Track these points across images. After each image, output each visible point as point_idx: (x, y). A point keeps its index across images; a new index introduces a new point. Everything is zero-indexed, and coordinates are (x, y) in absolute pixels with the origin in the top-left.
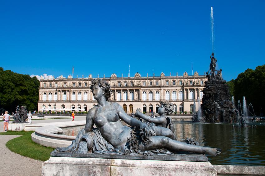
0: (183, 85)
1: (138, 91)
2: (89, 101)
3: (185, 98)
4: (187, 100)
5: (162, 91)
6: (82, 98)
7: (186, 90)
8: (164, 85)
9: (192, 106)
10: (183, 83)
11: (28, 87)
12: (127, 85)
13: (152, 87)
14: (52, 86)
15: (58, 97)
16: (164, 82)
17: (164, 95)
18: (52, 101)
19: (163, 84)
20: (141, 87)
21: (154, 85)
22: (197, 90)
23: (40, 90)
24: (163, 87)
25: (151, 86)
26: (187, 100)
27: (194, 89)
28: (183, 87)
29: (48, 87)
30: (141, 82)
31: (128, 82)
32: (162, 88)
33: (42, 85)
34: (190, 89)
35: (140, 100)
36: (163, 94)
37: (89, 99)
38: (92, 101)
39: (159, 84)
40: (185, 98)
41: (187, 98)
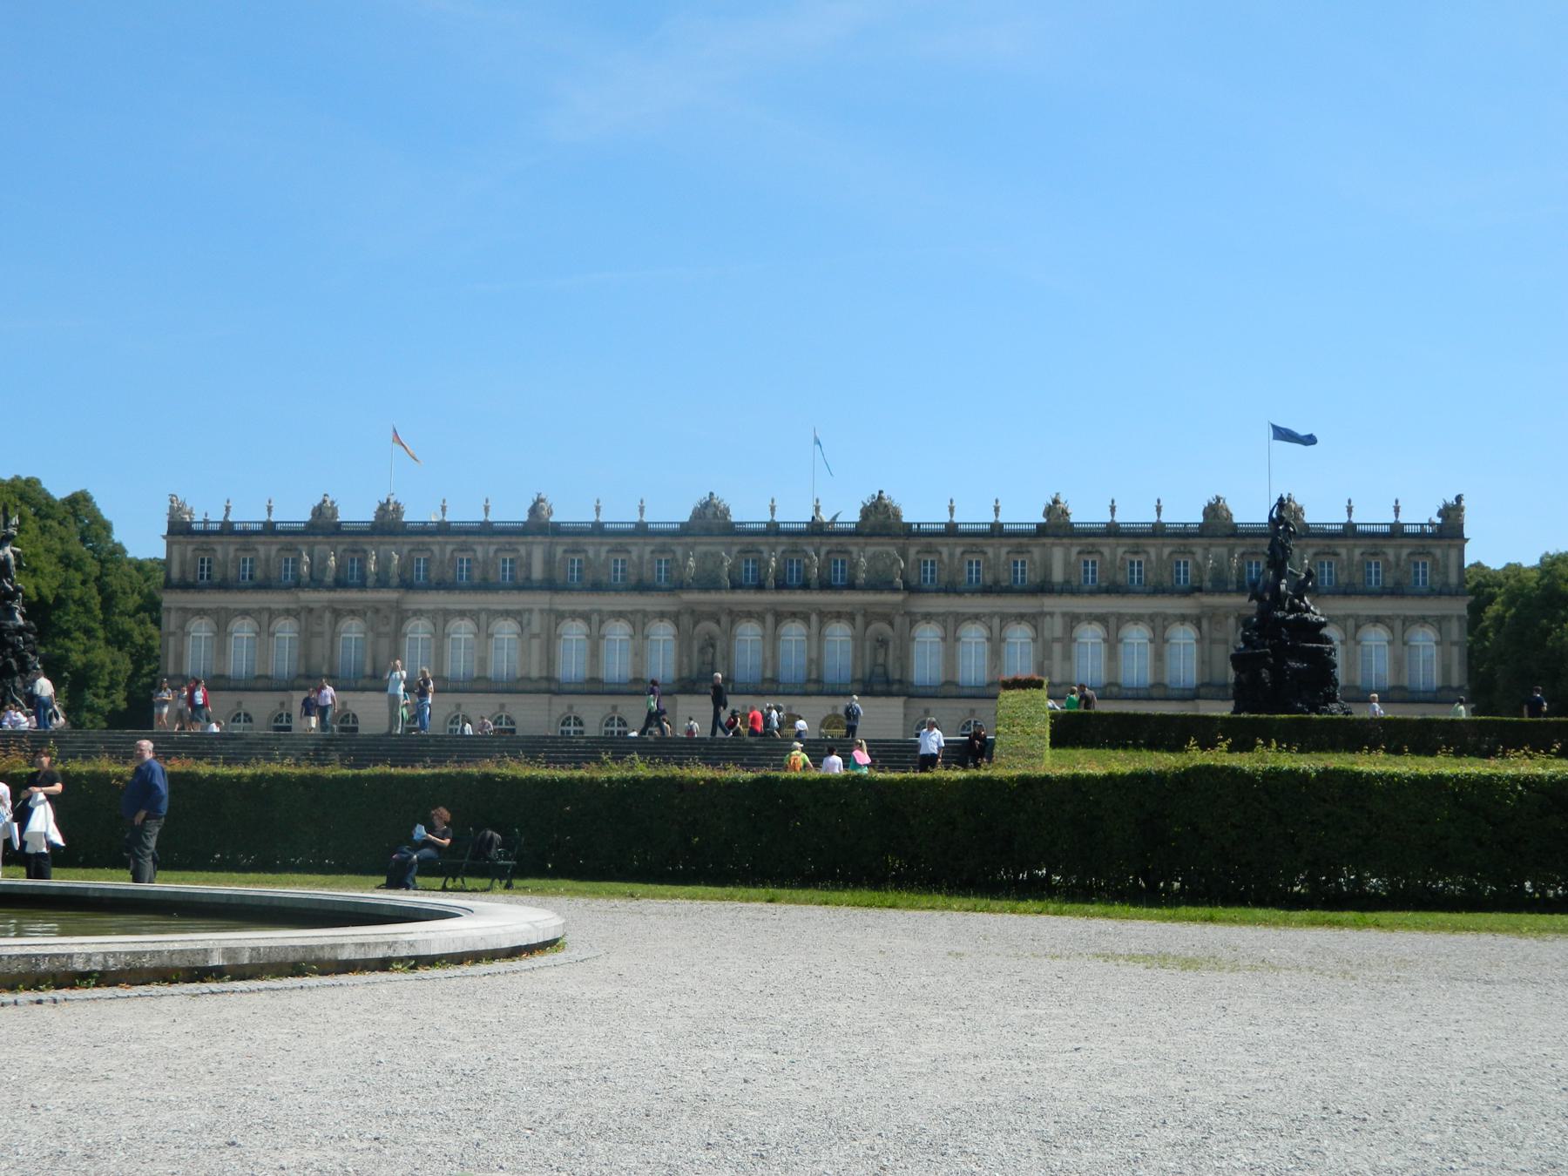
2: (529, 686)
6: (483, 662)
8: (1067, 582)
11: (55, 584)
13: (987, 590)
14: (259, 574)
15: (306, 654)
16: (1067, 563)
17: (1067, 656)
18: (260, 684)
19: (1058, 576)
21: (996, 582)
25: (974, 585)
29: (224, 579)
30: (904, 556)
32: (1051, 603)
33: (183, 563)
35: (895, 688)
36: (1057, 647)
37: (535, 673)
38: (553, 687)
39: (1033, 577)
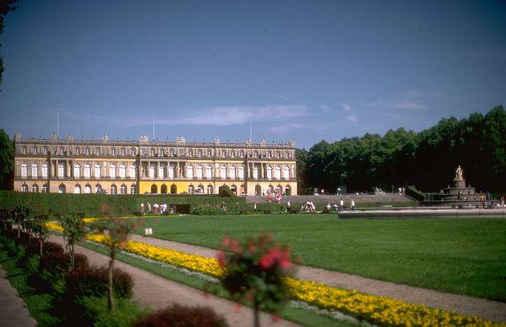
0: (246, 157)
1: (183, 164)
3: (249, 176)
4: (252, 179)
5: (217, 165)
7: (251, 164)
9: (258, 189)
10: (246, 155)
12: (156, 156)
20: (188, 158)
22: (264, 164)
23: (16, 158)
24: (219, 159)
26: (252, 179)
27: (260, 164)
28: (246, 159)
31: (167, 150)
34: (255, 164)
40: (249, 176)
41: (265, 176)
